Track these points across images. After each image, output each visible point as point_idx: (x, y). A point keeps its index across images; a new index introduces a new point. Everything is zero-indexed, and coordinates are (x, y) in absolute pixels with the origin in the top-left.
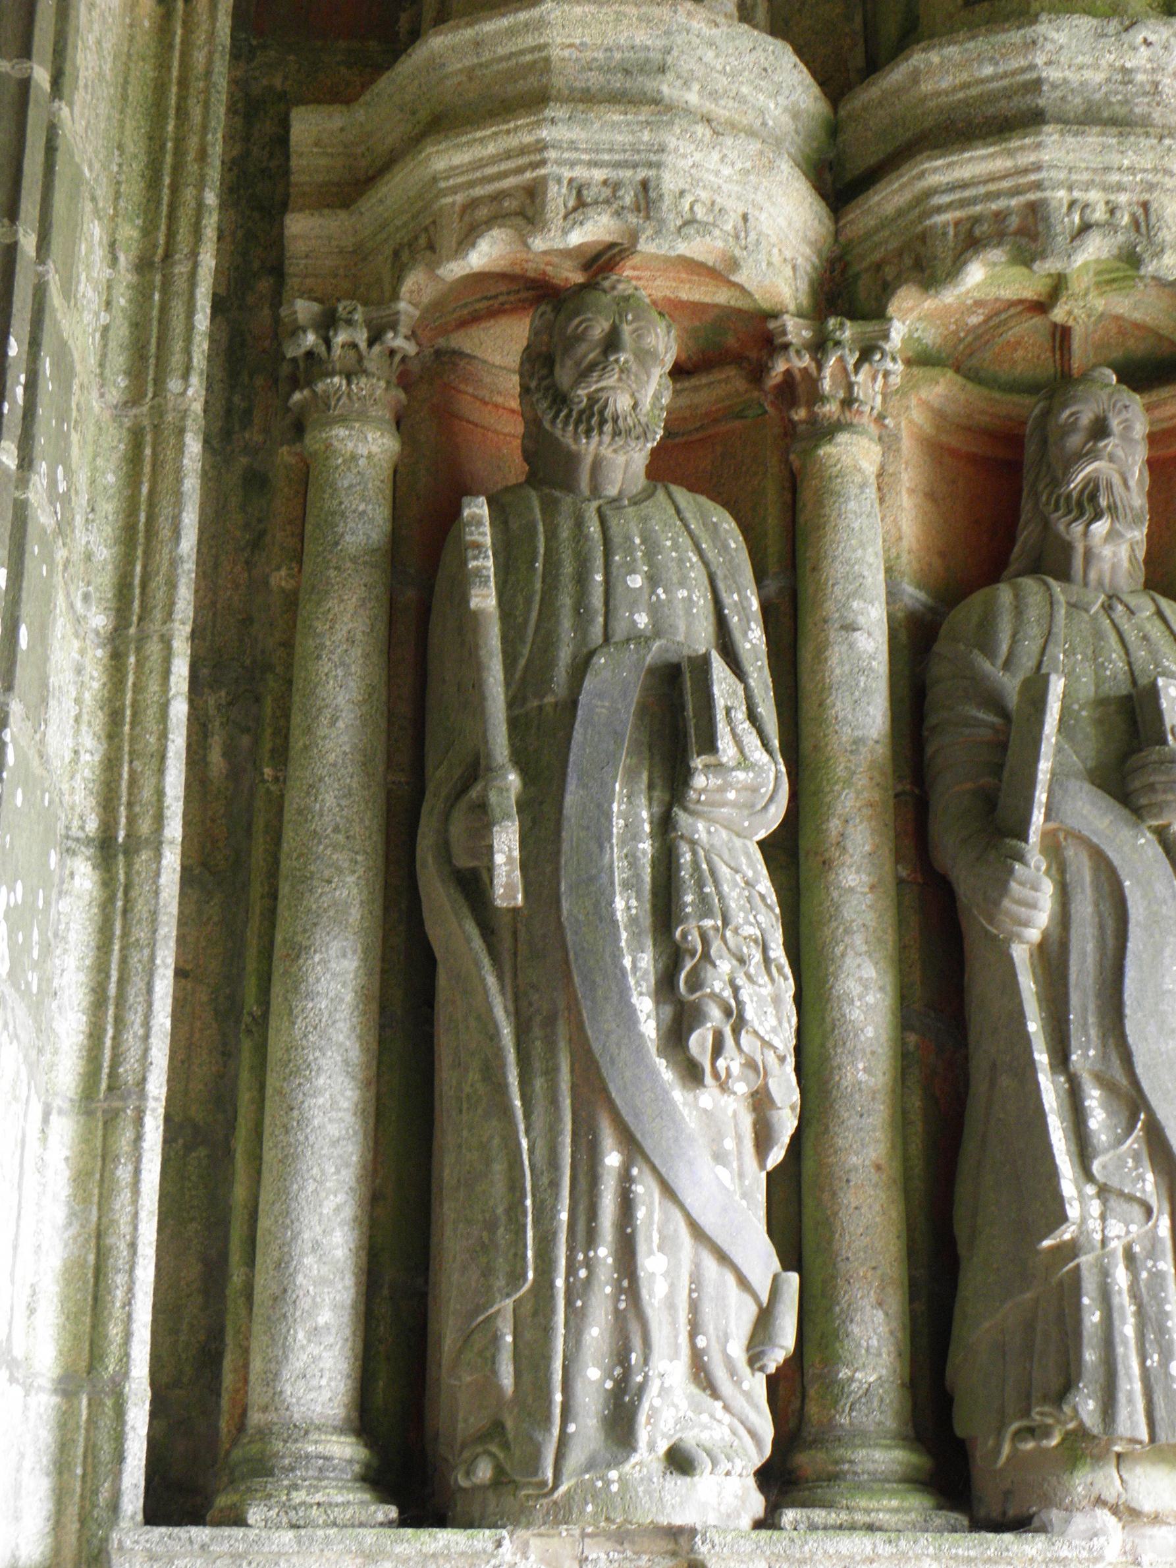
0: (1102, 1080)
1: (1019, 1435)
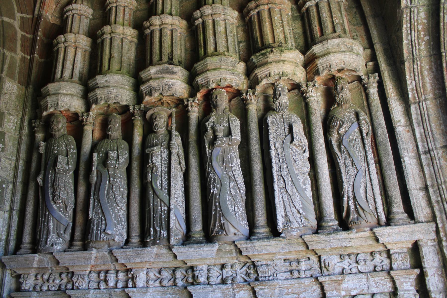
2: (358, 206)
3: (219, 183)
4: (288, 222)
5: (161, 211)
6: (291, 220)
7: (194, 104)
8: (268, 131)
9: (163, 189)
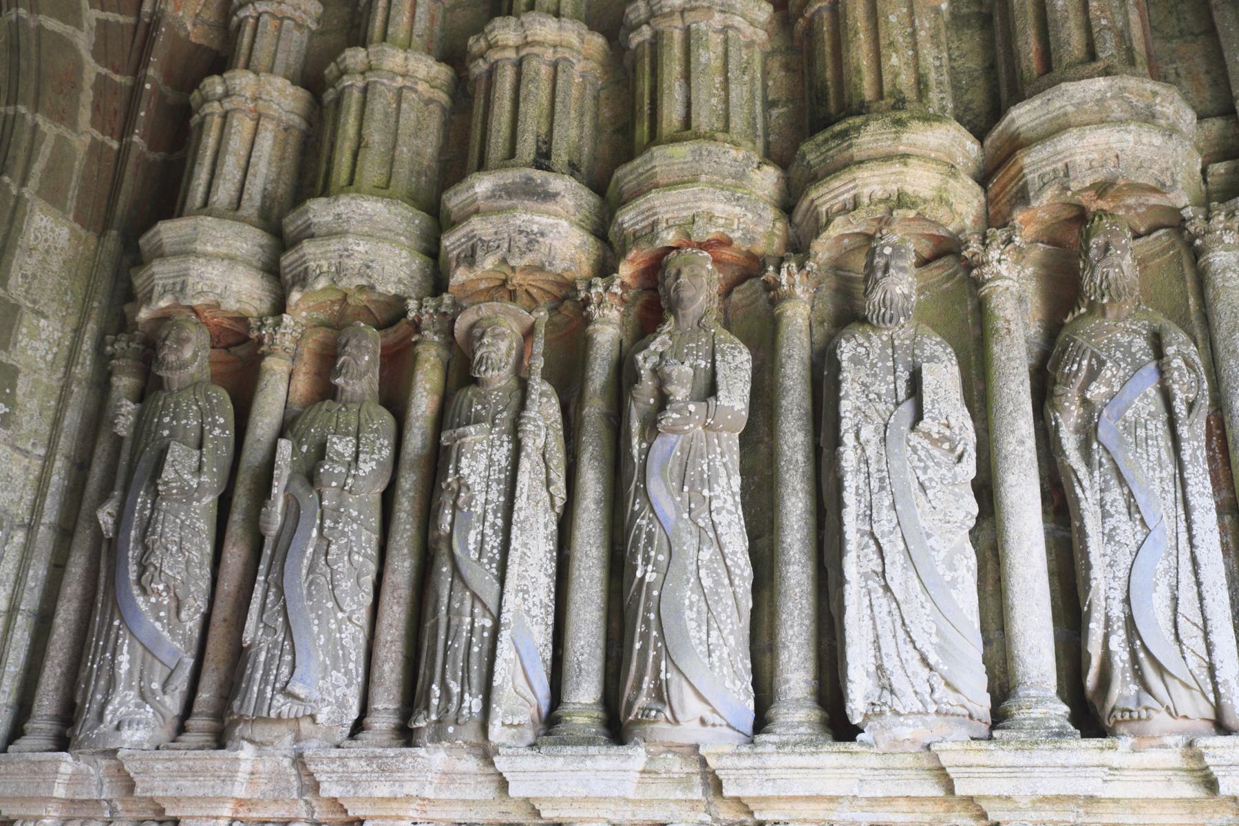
2: (1142, 655)
3: (666, 547)
4: (886, 693)
5: (472, 631)
6: (895, 686)
8: (837, 385)
9: (485, 561)
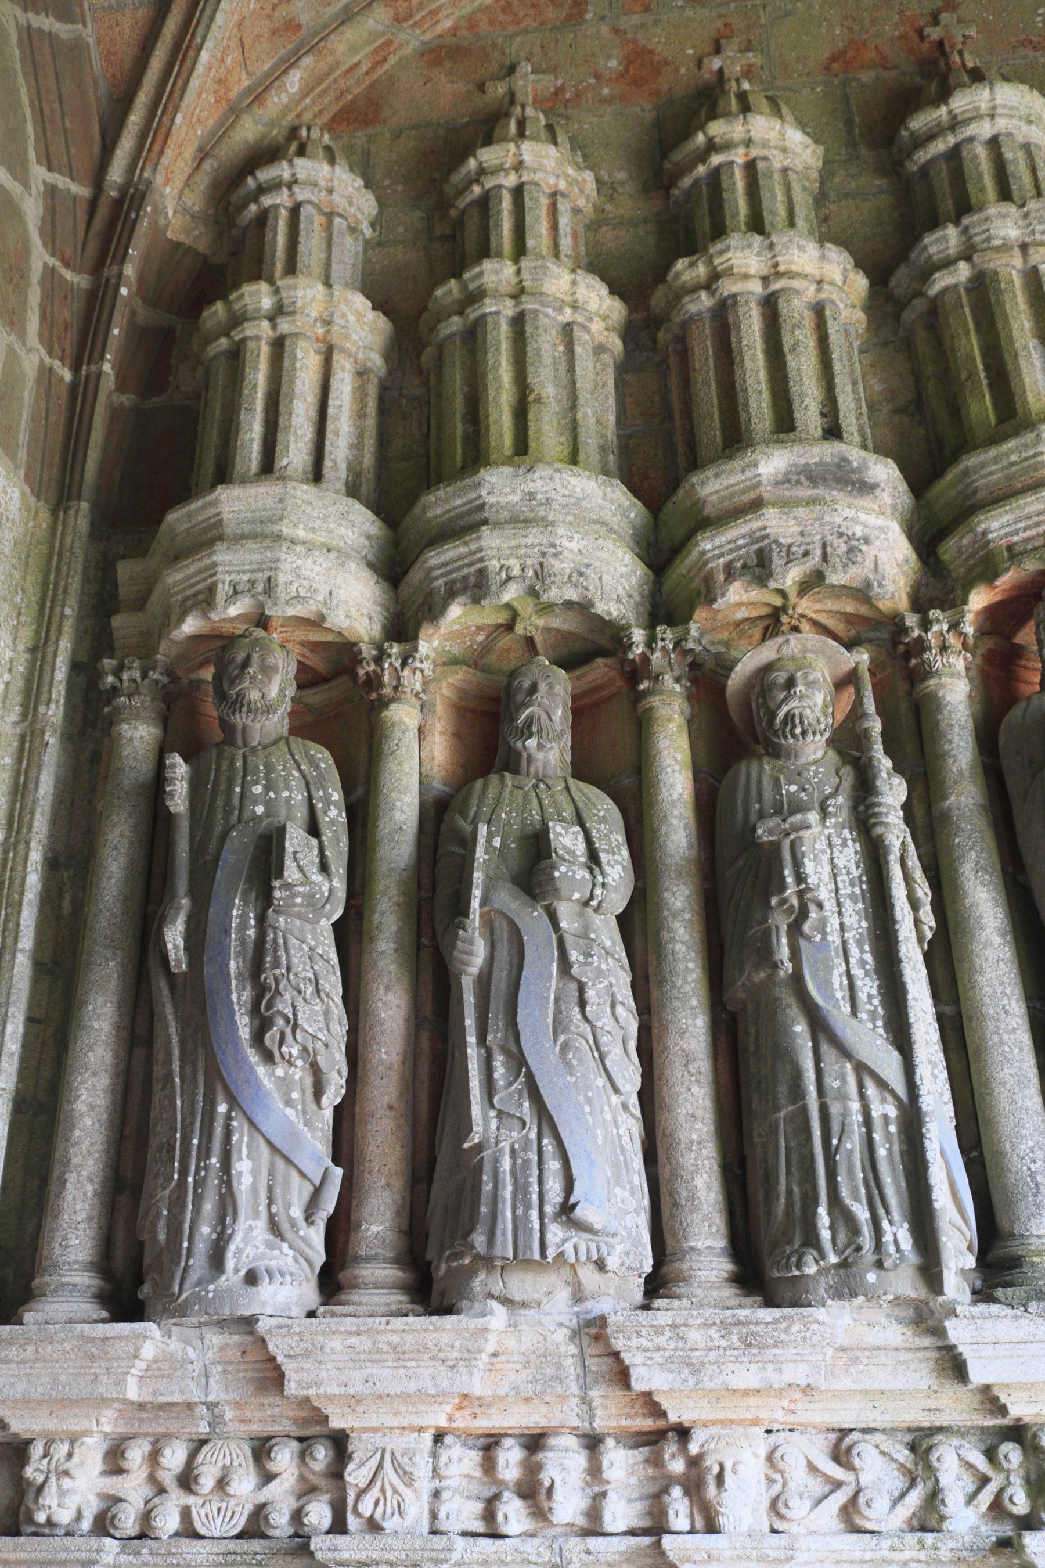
0: (505, 1051)
1: (448, 1260)
5: (868, 1122)
7: (952, 640)
